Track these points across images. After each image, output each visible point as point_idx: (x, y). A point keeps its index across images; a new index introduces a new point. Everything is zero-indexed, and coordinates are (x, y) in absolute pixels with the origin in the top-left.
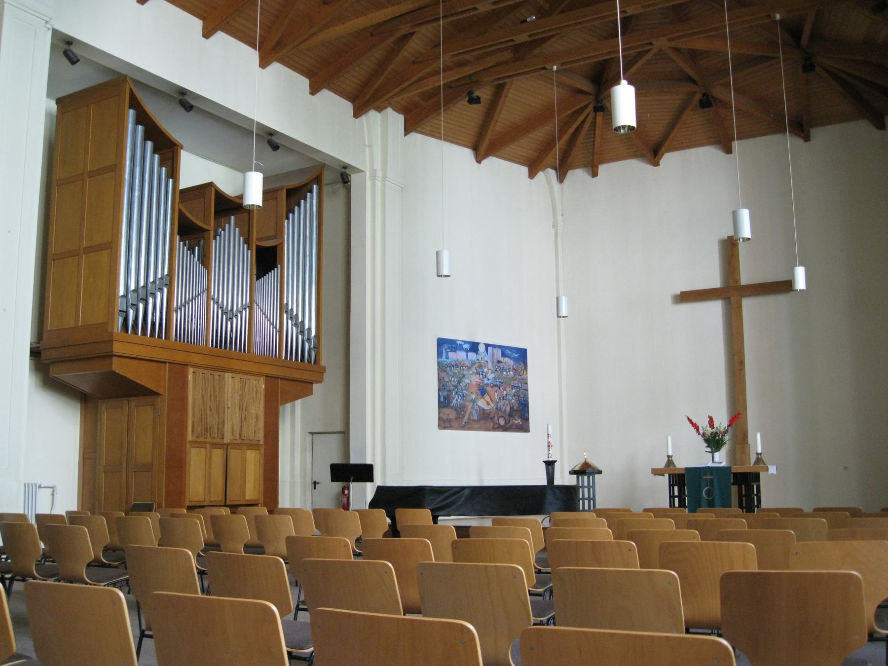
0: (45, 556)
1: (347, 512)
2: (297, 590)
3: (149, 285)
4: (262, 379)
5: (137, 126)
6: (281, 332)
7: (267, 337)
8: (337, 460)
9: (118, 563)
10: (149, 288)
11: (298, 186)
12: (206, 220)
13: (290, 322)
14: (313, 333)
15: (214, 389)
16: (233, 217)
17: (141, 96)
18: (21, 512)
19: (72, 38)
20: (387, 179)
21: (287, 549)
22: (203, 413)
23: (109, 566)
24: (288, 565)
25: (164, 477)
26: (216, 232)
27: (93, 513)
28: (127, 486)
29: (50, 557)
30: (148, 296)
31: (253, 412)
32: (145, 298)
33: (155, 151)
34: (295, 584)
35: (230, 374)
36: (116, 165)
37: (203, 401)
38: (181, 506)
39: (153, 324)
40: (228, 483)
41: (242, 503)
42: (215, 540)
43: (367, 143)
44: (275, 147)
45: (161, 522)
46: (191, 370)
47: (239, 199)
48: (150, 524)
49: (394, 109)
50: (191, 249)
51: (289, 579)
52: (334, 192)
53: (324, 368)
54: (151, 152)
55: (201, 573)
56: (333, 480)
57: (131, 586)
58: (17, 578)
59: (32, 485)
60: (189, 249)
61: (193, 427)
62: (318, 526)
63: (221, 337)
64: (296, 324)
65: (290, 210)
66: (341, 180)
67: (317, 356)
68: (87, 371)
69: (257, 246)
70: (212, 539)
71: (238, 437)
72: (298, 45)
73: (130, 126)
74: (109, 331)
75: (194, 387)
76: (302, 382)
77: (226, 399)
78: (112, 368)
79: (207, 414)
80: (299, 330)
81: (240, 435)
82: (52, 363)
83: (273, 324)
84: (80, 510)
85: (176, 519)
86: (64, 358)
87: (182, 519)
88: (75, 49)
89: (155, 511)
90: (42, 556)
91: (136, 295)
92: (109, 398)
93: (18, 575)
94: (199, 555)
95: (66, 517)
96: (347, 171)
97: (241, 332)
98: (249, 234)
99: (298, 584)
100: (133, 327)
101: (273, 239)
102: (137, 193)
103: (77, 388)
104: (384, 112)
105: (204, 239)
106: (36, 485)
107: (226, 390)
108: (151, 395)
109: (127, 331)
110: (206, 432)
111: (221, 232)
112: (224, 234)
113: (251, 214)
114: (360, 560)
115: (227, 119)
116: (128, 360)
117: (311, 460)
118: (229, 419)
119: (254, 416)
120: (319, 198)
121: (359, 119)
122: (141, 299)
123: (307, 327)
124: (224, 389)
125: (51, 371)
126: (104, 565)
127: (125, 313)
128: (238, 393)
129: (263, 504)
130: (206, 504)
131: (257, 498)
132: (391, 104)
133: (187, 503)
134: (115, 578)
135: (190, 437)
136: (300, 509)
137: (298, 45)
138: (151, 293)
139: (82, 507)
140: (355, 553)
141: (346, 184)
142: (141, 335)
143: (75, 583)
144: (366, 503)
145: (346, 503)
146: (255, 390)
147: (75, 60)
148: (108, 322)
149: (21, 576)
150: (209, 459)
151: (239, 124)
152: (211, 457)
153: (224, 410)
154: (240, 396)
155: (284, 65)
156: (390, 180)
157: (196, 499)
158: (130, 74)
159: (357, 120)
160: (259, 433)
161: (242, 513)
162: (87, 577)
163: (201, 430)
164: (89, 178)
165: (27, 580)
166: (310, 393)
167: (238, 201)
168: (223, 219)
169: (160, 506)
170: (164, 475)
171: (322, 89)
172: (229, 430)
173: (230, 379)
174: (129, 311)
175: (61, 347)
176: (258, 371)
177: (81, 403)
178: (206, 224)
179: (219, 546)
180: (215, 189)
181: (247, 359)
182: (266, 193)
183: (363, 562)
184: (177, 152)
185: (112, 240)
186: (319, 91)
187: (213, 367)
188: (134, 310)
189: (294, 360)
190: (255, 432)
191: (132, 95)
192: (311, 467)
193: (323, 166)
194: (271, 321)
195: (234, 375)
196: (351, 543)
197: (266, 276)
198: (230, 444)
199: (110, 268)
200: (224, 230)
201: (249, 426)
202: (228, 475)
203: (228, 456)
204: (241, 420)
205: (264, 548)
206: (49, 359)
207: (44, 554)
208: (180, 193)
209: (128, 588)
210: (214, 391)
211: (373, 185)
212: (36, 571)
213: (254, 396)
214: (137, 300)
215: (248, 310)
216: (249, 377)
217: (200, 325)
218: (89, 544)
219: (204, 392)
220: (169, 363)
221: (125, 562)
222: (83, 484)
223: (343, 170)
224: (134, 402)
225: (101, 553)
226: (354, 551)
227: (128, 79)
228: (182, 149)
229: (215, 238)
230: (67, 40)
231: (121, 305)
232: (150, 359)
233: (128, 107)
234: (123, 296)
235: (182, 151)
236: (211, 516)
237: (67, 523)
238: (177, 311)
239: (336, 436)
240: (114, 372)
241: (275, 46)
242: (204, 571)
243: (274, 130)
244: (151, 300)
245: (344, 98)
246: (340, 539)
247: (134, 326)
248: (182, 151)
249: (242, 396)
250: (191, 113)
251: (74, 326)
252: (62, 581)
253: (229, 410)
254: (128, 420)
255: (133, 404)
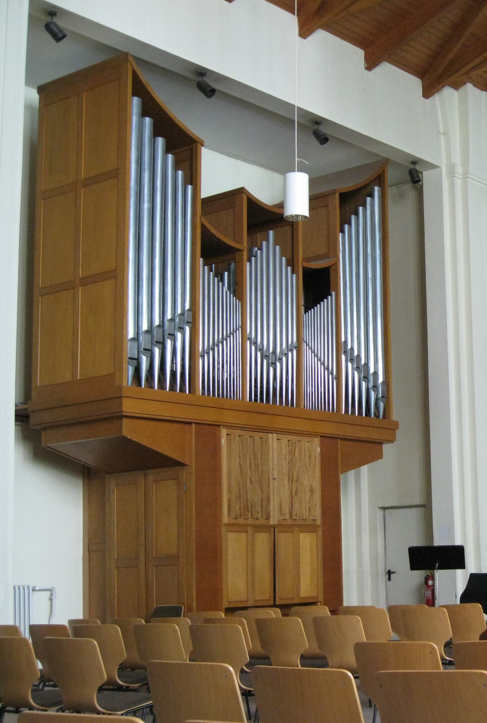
0: (44, 679)
1: (432, 608)
2: (370, 712)
3: (167, 323)
4: (317, 441)
5: (144, 118)
6: (338, 378)
7: (321, 386)
8: (417, 542)
9: (138, 685)
10: (166, 327)
11: (354, 188)
12: (238, 238)
13: (350, 365)
14: (381, 379)
15: (254, 455)
16: (271, 233)
17: (146, 78)
18: (11, 622)
19: (56, 7)
20: (469, 176)
21: (357, 660)
22: (241, 487)
23: (127, 689)
24: (358, 680)
25: (194, 571)
26: (250, 251)
27: (104, 622)
28: (147, 585)
29: (50, 680)
30: (166, 338)
31: (306, 483)
32: (162, 341)
33: (168, 150)
34: (369, 704)
35: (275, 435)
36: (118, 169)
37: (242, 472)
38: (216, 607)
39: (173, 374)
40: (277, 577)
41: (296, 601)
42: (262, 650)
43: (442, 131)
44: (323, 139)
45: (192, 629)
46: (224, 432)
47: (279, 208)
48: (177, 633)
49: (474, 85)
50: (219, 275)
51: (360, 698)
52: (402, 195)
53: (397, 424)
54: (163, 151)
55: (246, 694)
56: (412, 568)
57: (156, 715)
58: (8, 708)
59: (24, 588)
60: (216, 275)
61: (229, 505)
62: (395, 627)
63: (262, 387)
64: (358, 368)
65: (345, 220)
66: (409, 178)
67: (386, 408)
68: (90, 438)
69: (304, 268)
70: (259, 648)
71: (287, 517)
72: (348, 7)
73: (135, 119)
74: (116, 385)
75: (229, 454)
76: (368, 442)
77: (271, 469)
78: (121, 431)
79: (246, 489)
80: (362, 375)
81: (291, 514)
82: (44, 429)
83: (328, 369)
84: (87, 618)
85: (211, 625)
86: (60, 421)
87: (218, 624)
88: (60, 22)
89: (184, 616)
90: (40, 679)
91: (150, 337)
92: (119, 472)
93: (10, 706)
94: (242, 671)
95: (68, 628)
96: (418, 167)
97: (287, 381)
98: (293, 254)
99: (373, 704)
100: (147, 379)
101: (324, 259)
102: (146, 206)
103: (77, 460)
104: (463, 88)
105: (235, 262)
106: (28, 588)
107: (271, 456)
108: (173, 466)
109: (140, 385)
110: (246, 512)
111: (256, 252)
112: (261, 255)
113: (295, 227)
114: (451, 670)
115: (260, 105)
116: (142, 422)
117: (383, 544)
118: (276, 494)
119: (308, 489)
120: (382, 204)
121: (431, 99)
122: (157, 342)
123: (372, 370)
124: (268, 454)
125: (43, 439)
126: (120, 689)
127: (136, 362)
128: (285, 460)
129: (323, 603)
130: (250, 604)
131: (314, 594)
132: (470, 78)
133: (225, 605)
134: (136, 704)
135: (225, 519)
136: (372, 607)
137: (348, 7)
138: (169, 334)
139: (90, 613)
140: (444, 662)
141: (416, 185)
142: (158, 388)
143: (84, 713)
144: (456, 596)
145: (431, 597)
146: (307, 454)
147: (60, 35)
148: (114, 373)
149: (13, 706)
150: (251, 546)
151: (275, 111)
152: (253, 545)
153: (269, 482)
154: (289, 463)
155: (331, 32)
156: (473, 177)
157: (236, 598)
158: (134, 52)
159: (428, 101)
160: (315, 511)
161: (297, 614)
162: (98, 702)
163: (240, 508)
164: (83, 187)
165: (22, 711)
166: (379, 456)
167: (277, 210)
168: (259, 235)
169: (189, 609)
170: (194, 568)
171: (381, 62)
172: (277, 507)
173: (275, 442)
174: (142, 358)
175: (56, 408)
176: (311, 430)
177: (83, 480)
178: (237, 242)
179: (268, 658)
180: (248, 197)
181: (296, 416)
182: (312, 199)
183: (455, 672)
184: (197, 150)
185: (116, 266)
186: (377, 65)
187: (253, 427)
188: (147, 357)
189: (357, 414)
190: (310, 508)
191: (136, 78)
192: (383, 553)
193: (386, 162)
194: (326, 364)
195: (280, 436)
196: (439, 649)
197: (316, 306)
198: (278, 525)
199: (115, 303)
200: (261, 249)
201: (301, 502)
202: (276, 566)
203: (276, 541)
204: (291, 494)
205: (327, 659)
206: (41, 424)
207: (42, 677)
208: (202, 204)
209: (152, 718)
210: (254, 457)
211: (452, 185)
212: (33, 698)
213: (307, 463)
214: (152, 344)
215: (295, 351)
216: (300, 438)
217: (234, 372)
218: (100, 662)
219: (242, 460)
220: (196, 423)
221: (147, 684)
222: (90, 584)
223: (412, 166)
224: (152, 475)
225: (116, 672)
226: (443, 659)
227: (130, 58)
228: (202, 146)
229: (249, 260)
230: (49, 10)
231: (130, 350)
232: (170, 419)
233: (131, 94)
234: (133, 339)
235: (202, 148)
236: (257, 620)
237: (71, 636)
238: (203, 356)
239: (414, 511)
240: (125, 438)
241: (319, 8)
242: (250, 691)
243: (321, 117)
244: (169, 344)
245: (410, 73)
246: (425, 644)
247: (149, 377)
248: (202, 148)
249: (291, 464)
250: (213, 99)
251: (70, 379)
252: (66, 711)
253: (275, 482)
254: (145, 500)
255: (151, 478)
